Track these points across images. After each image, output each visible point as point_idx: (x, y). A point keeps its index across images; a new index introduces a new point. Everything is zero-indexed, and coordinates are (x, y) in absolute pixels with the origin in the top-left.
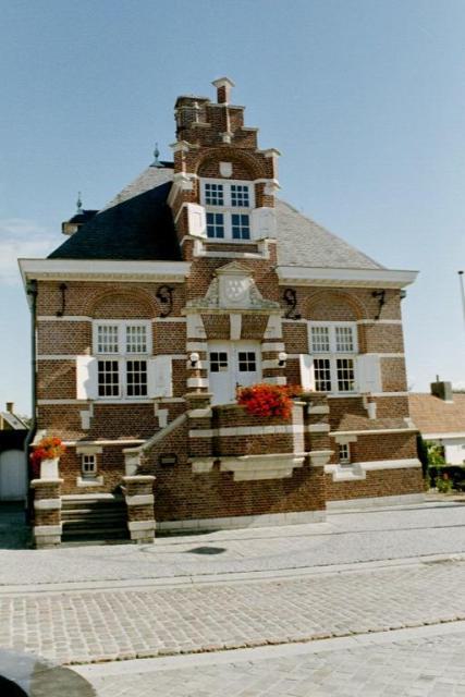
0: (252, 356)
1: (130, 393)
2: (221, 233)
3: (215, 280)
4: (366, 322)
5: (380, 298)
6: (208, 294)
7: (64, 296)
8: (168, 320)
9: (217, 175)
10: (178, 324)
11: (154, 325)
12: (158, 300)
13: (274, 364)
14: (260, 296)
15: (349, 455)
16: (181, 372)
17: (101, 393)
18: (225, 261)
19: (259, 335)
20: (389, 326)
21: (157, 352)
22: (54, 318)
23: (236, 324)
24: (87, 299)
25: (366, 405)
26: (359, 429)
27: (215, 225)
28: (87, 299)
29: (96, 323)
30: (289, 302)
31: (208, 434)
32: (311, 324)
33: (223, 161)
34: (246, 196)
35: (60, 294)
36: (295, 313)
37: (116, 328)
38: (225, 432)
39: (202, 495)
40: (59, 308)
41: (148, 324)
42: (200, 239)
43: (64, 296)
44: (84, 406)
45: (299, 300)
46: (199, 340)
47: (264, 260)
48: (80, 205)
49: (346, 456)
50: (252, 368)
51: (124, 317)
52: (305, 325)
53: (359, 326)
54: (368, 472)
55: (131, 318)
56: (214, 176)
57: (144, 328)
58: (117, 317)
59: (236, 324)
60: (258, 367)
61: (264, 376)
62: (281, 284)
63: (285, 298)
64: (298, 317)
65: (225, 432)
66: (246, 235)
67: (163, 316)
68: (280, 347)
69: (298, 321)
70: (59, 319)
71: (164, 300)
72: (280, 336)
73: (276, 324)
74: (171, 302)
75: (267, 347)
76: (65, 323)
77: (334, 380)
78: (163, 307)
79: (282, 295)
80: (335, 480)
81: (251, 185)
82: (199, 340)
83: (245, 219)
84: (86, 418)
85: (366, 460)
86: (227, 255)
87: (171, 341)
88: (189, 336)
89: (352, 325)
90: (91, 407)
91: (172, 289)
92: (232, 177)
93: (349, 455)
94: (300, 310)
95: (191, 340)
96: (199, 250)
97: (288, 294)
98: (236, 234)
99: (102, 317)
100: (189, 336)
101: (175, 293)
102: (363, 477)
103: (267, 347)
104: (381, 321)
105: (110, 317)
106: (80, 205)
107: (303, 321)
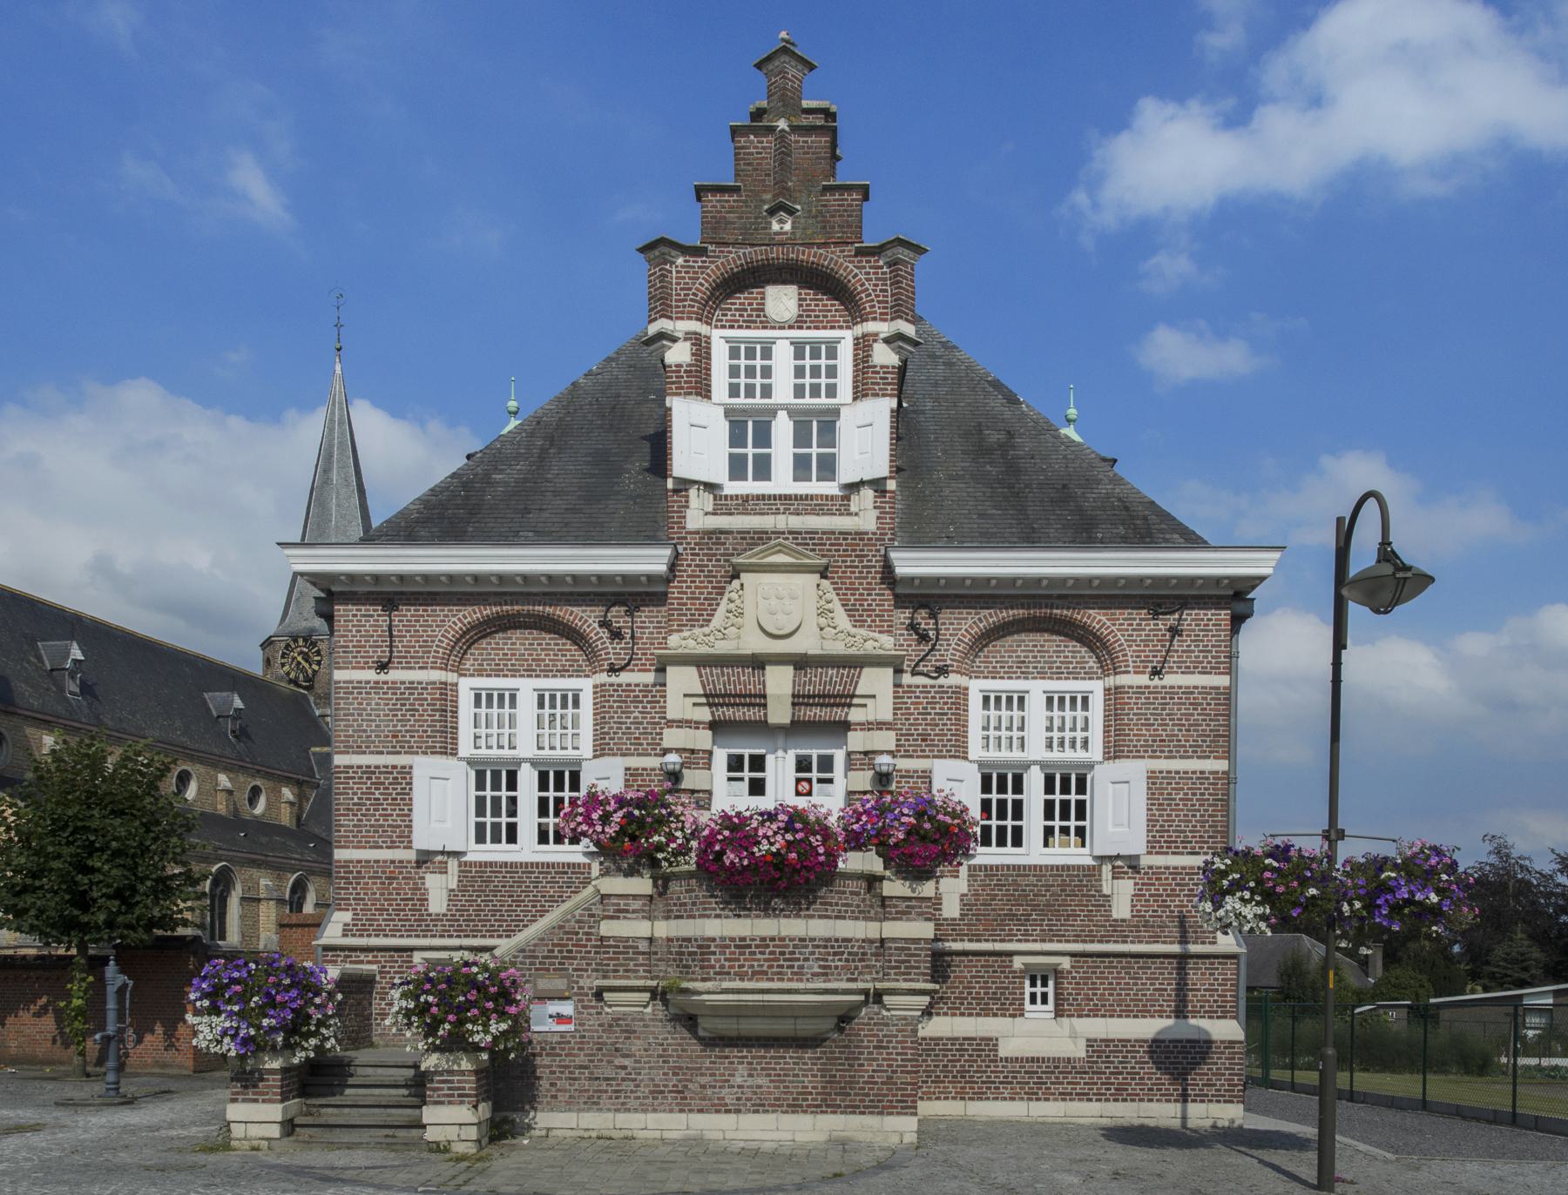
2: (763, 469)
3: (736, 583)
4: (1123, 680)
6: (717, 621)
8: (624, 678)
11: (599, 690)
14: (842, 620)
18: (760, 537)
20: (1189, 690)
22: (370, 675)
29: (466, 687)
30: (923, 638)
33: (775, 282)
34: (832, 372)
35: (383, 621)
37: (513, 698)
40: (382, 653)
41: (585, 686)
42: (710, 487)
43: (390, 627)
46: (696, 725)
51: (530, 673)
52: (962, 692)
53: (1107, 690)
58: (514, 673)
62: (899, 590)
63: (913, 627)
64: (942, 671)
66: (828, 468)
67: (613, 670)
68: (887, 740)
69: (942, 681)
70: (382, 677)
71: (616, 635)
72: (889, 717)
74: (633, 637)
78: (613, 651)
81: (846, 340)
82: (696, 725)
88: (671, 714)
89: (1096, 689)
92: (799, 324)
94: (949, 651)
95: (671, 723)
96: (698, 515)
98: (801, 467)
99: (480, 673)
100: (671, 714)
104: (1170, 680)
105: (498, 673)
107: (953, 679)
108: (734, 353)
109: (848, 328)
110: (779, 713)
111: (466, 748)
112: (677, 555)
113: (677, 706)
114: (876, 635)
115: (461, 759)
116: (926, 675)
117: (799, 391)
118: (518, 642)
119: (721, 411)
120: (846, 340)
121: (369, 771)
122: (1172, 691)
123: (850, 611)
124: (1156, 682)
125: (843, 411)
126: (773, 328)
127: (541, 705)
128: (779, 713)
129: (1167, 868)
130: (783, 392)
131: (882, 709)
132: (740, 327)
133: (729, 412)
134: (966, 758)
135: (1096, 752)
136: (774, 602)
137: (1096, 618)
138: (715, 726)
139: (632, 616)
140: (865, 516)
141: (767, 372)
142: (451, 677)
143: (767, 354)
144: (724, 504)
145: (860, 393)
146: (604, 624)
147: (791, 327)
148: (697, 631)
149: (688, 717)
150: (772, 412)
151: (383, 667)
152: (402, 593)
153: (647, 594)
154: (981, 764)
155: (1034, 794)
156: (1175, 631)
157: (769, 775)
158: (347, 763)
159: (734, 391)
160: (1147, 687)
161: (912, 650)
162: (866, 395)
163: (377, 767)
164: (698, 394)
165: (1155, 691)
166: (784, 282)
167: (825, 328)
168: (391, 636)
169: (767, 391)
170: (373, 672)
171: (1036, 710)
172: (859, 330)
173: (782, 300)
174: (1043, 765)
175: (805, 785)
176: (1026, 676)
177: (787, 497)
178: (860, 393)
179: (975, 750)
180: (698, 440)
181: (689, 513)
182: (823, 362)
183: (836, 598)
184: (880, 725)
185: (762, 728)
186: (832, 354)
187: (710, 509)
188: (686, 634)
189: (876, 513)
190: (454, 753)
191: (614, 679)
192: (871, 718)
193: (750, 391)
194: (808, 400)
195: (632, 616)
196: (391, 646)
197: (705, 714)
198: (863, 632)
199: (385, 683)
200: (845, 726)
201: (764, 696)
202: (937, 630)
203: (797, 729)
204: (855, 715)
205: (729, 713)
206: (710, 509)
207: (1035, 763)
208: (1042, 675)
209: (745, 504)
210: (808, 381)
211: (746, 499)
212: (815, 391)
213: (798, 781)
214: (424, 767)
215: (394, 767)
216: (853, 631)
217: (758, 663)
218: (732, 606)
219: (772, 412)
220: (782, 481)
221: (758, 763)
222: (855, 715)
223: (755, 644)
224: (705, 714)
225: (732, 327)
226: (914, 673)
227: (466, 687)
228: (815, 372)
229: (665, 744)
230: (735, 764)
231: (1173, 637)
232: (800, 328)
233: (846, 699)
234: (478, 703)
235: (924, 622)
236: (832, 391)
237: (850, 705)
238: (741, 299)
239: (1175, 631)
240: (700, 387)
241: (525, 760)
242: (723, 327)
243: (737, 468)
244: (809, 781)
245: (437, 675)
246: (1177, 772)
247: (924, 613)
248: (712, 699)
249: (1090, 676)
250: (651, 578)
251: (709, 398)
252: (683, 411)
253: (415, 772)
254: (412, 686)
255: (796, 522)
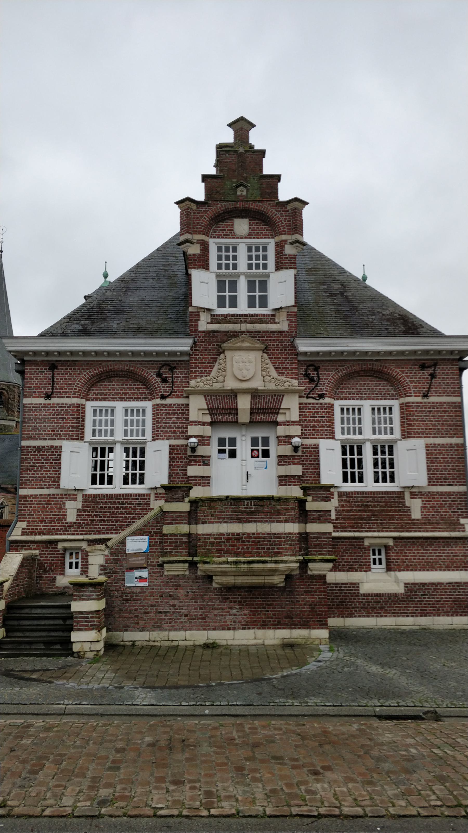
0: (266, 441)
1: (126, 482)
2: (234, 303)
3: (222, 355)
5: (431, 370)
6: (213, 373)
7: (53, 377)
8: (169, 401)
9: (231, 234)
10: (179, 406)
12: (159, 380)
13: (287, 450)
14: (274, 373)
15: (384, 561)
16: (181, 458)
17: (94, 482)
18: (233, 335)
19: (272, 417)
20: (441, 404)
21: (156, 437)
22: (42, 401)
23: (244, 404)
24: (82, 377)
25: (408, 502)
26: (396, 530)
27: (227, 294)
28: (82, 377)
29: (90, 406)
30: (312, 380)
31: (185, 529)
32: (338, 404)
34: (265, 258)
35: (49, 374)
36: (317, 391)
38: (203, 529)
39: (176, 602)
40: (48, 390)
41: (148, 405)
42: (209, 310)
43: (53, 377)
44: (70, 495)
45: (323, 377)
46: (203, 424)
47: (280, 332)
48: (106, 276)
49: (380, 563)
50: (266, 454)
51: (121, 399)
52: (331, 406)
53: (401, 405)
54: (407, 585)
55: (129, 399)
56: (226, 237)
57: (144, 411)
58: (114, 399)
59: (244, 404)
60: (273, 454)
61: (279, 464)
62: (300, 358)
63: (307, 375)
64: (321, 396)
65: (203, 529)
66: (264, 302)
67: (163, 397)
68: (297, 430)
69: (321, 401)
70: (48, 402)
71: (164, 380)
73: (291, 407)
74: (173, 382)
75: (281, 431)
76: (53, 406)
77: (368, 470)
79: (302, 371)
80: (362, 591)
82: (203, 424)
83: (264, 285)
84: (72, 510)
85: (407, 569)
86: (237, 327)
87: (170, 423)
88: (191, 419)
89: (395, 404)
90: (80, 498)
91: (175, 368)
92: (250, 236)
93: (384, 561)
94: (324, 387)
96: (204, 324)
97: (311, 368)
98: (251, 304)
99: (96, 399)
100: (191, 419)
101: (177, 372)
102: (400, 589)
103: (281, 431)
104: (432, 399)
105: (105, 399)
106: (106, 276)
107: (327, 400)
108: (220, 249)
109: (273, 238)
110: (244, 417)
111: (88, 436)
112: (195, 343)
113: (194, 415)
114: (289, 379)
115: (85, 442)
116: (314, 398)
117: (250, 267)
118: (116, 385)
119: (214, 276)
120: (271, 244)
121: (39, 448)
122: (433, 404)
123: (277, 369)
124: (425, 400)
125: (271, 275)
126: (238, 238)
127: (126, 414)
128: (244, 417)
129: (437, 492)
130: (242, 266)
131: (295, 415)
132: (222, 238)
133: (218, 276)
134: (334, 439)
135: (397, 434)
136: (241, 365)
137: (395, 371)
138: (212, 424)
139: (172, 371)
140: (283, 325)
141: (235, 258)
142: (83, 401)
143: (235, 249)
144: (215, 319)
145: (279, 267)
146: (159, 375)
147: (246, 238)
148: (204, 378)
149: (200, 420)
150: (238, 276)
151: (48, 397)
152: (59, 361)
153: (180, 361)
154: (342, 441)
155: (368, 457)
156: (433, 376)
157: (238, 448)
158: (28, 445)
159: (220, 266)
160: (421, 403)
161: (306, 387)
162: (282, 268)
163: (43, 447)
164: (203, 268)
165: (425, 405)
166: (243, 217)
167: (261, 238)
168: (53, 381)
169: (235, 267)
170: (43, 399)
171: (367, 415)
172: (278, 239)
173: (242, 226)
174: (371, 441)
175: (256, 452)
176: (361, 398)
177: (245, 315)
178: (279, 267)
179: (338, 435)
180: (204, 290)
181: (200, 323)
182: (261, 253)
183: (270, 362)
184: (293, 423)
185: (236, 423)
186: (265, 249)
187: (209, 321)
188: (199, 380)
189: (287, 322)
190: (82, 439)
191: (163, 402)
192: (288, 419)
193: (227, 267)
194: (254, 270)
195: (172, 371)
196: (53, 386)
197: (208, 419)
198: (283, 378)
199: (49, 404)
200: (276, 423)
201: (237, 409)
202: (318, 377)
203: (253, 423)
204: (280, 418)
205: (220, 418)
206: (209, 321)
207: (368, 440)
208: (369, 398)
209: (226, 319)
210: (254, 262)
211: (226, 316)
212: (257, 266)
213: (252, 450)
214: (68, 446)
215: (52, 446)
216: (279, 377)
217: (234, 394)
218: (220, 366)
219: (238, 276)
220: (242, 308)
221: (233, 441)
222: (280, 418)
223: (231, 384)
224: (208, 419)
225: (218, 238)
226: (308, 397)
227: (90, 406)
228: (257, 258)
229: (189, 433)
230: (221, 442)
231: (432, 379)
232: (250, 238)
233: (276, 411)
234: (95, 414)
235: (313, 374)
236: (265, 266)
237: (278, 413)
238: (222, 225)
239: (433, 376)
240: (204, 264)
241: (118, 442)
242: (214, 237)
243: (221, 302)
244: (258, 450)
245: (75, 401)
246: (439, 444)
247: (311, 368)
248: (211, 411)
249: (392, 398)
250: (182, 353)
251: (208, 270)
252: (197, 275)
253: (63, 449)
254: (62, 406)
255: (249, 327)
